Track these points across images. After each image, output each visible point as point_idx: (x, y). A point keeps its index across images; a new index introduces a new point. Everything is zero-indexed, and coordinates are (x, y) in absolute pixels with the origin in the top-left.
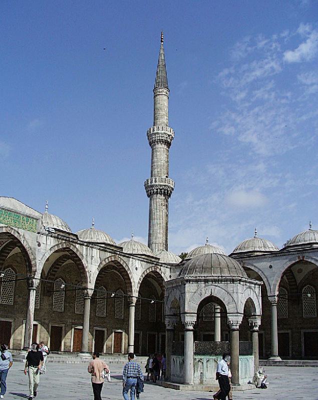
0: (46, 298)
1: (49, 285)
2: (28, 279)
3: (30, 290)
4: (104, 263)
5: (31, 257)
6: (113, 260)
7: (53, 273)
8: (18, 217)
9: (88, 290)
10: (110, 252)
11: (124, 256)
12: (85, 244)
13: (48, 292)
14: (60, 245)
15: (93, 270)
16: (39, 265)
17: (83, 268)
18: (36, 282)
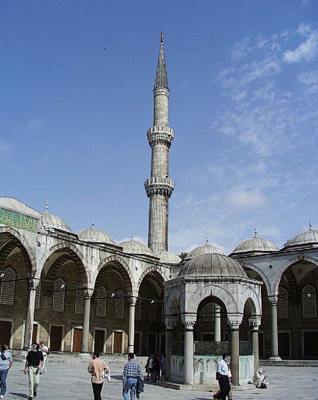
0: (46, 298)
1: (49, 285)
2: (28, 279)
3: (30, 290)
4: (104, 263)
5: (31, 257)
6: (113, 260)
7: (53, 273)
8: (18, 217)
9: (88, 290)
10: (110, 252)
11: (124, 256)
12: (85, 244)
13: (48, 292)
14: (60, 245)
15: (93, 270)
16: (39, 265)
17: (83, 268)
18: (36, 282)
